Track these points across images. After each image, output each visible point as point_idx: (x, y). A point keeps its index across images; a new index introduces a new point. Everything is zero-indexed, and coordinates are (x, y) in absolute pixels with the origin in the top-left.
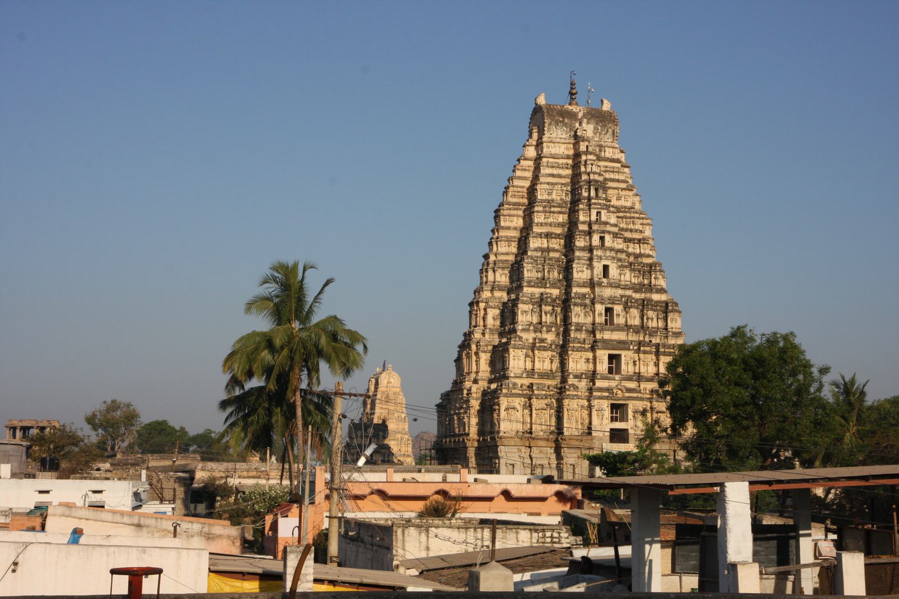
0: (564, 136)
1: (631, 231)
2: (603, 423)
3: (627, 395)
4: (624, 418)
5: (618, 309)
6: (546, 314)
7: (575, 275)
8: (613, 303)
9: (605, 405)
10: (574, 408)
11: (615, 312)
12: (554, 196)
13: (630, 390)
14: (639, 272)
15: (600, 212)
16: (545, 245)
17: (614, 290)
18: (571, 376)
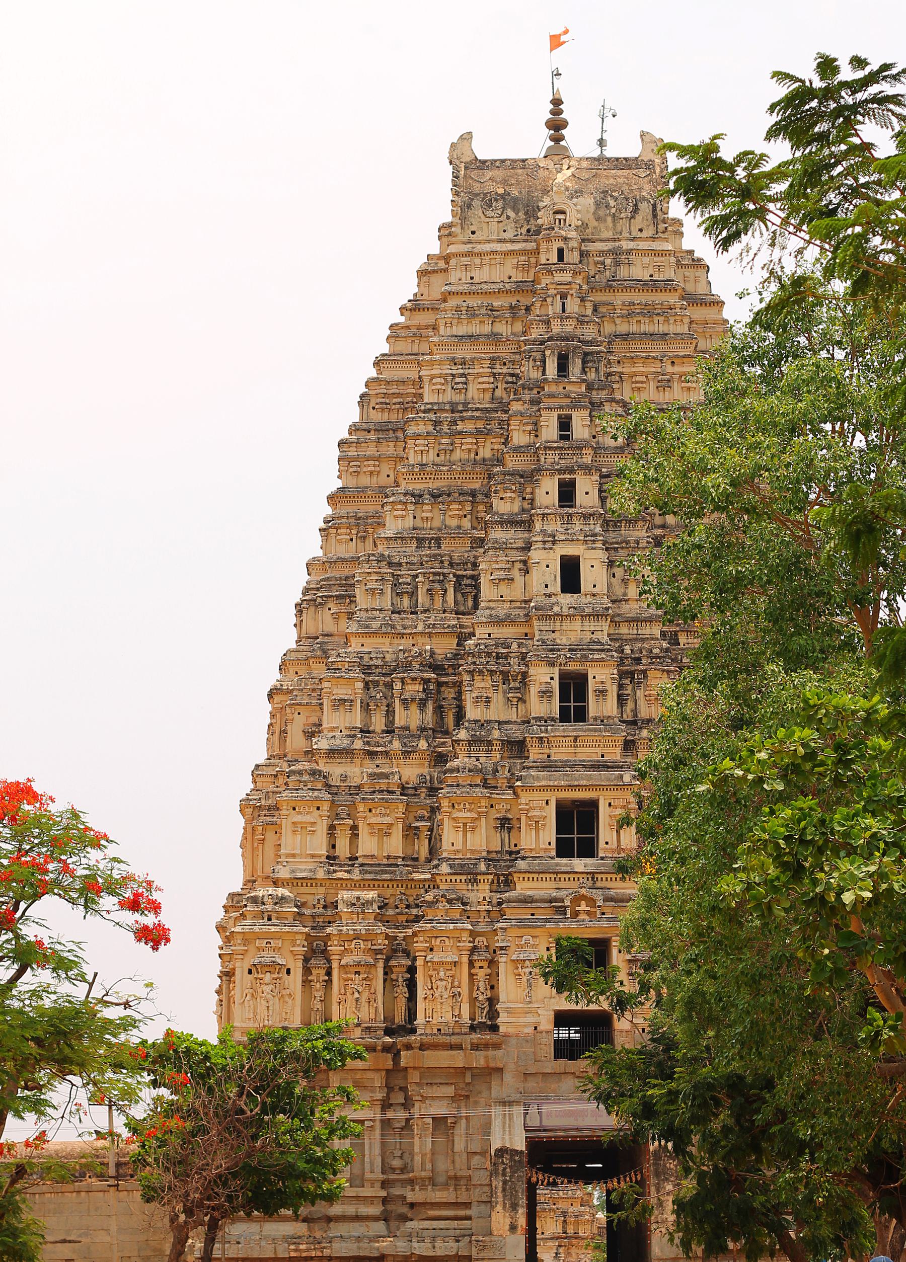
0: (509, 235)
5: (601, 676)
6: (405, 703)
7: (487, 592)
10: (442, 951)
15: (570, 417)
16: (437, 523)
18: (445, 868)
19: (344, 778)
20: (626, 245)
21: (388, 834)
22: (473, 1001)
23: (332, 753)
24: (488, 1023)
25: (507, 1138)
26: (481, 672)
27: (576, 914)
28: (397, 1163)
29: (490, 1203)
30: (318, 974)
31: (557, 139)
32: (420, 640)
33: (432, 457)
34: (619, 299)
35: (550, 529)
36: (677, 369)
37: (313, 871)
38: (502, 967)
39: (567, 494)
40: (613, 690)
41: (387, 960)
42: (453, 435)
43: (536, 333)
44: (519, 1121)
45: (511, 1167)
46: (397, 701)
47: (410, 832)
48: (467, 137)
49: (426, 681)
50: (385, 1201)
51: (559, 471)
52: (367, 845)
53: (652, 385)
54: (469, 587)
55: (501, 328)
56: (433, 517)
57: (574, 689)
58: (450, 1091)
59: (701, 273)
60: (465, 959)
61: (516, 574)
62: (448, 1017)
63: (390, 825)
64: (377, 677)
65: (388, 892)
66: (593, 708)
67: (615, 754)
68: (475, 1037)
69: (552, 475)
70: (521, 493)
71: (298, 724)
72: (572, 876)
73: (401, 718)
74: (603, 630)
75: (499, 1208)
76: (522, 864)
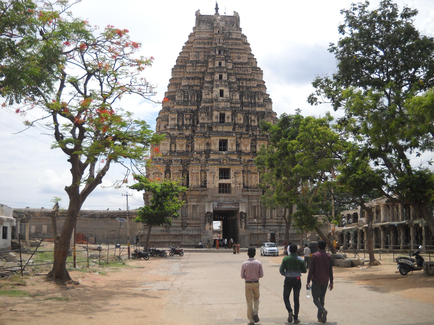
0: (208, 28)
1: (245, 74)
2: (214, 181)
3: (230, 163)
5: (228, 114)
6: (186, 119)
7: (204, 96)
8: (225, 110)
9: (216, 170)
10: (194, 170)
11: (226, 116)
12: (200, 58)
13: (233, 160)
14: (248, 96)
15: (221, 62)
16: (193, 84)
17: (226, 104)
18: (195, 153)
19: (173, 134)
20: (231, 31)
21: (183, 146)
22: (201, 181)
23: (171, 129)
24: (204, 185)
26: (203, 113)
27: (223, 163)
28: (184, 215)
29: (205, 224)
30: (168, 175)
31: (217, 11)
32: (189, 107)
33: (192, 71)
34: (230, 41)
35: (218, 84)
36: (242, 55)
37: (167, 153)
38: (207, 174)
39: (221, 77)
40: (231, 117)
41: (182, 173)
43: (214, 46)
44: (212, 206)
47: (187, 146)
48: (199, 11)
49: (191, 115)
50: (182, 223)
51: (219, 73)
52: (178, 148)
53: (237, 58)
54: (200, 96)
55: (206, 46)
56: (191, 82)
57: (222, 116)
58: (196, 200)
59: (245, 38)
60: (200, 172)
61: (210, 93)
62: (196, 184)
63: (183, 144)
64: (180, 114)
65: (182, 158)
66: (226, 121)
67: (231, 130)
68: (202, 189)
70: (211, 77)
71: (163, 124)
74: (229, 105)
75: (207, 224)
76: (212, 152)
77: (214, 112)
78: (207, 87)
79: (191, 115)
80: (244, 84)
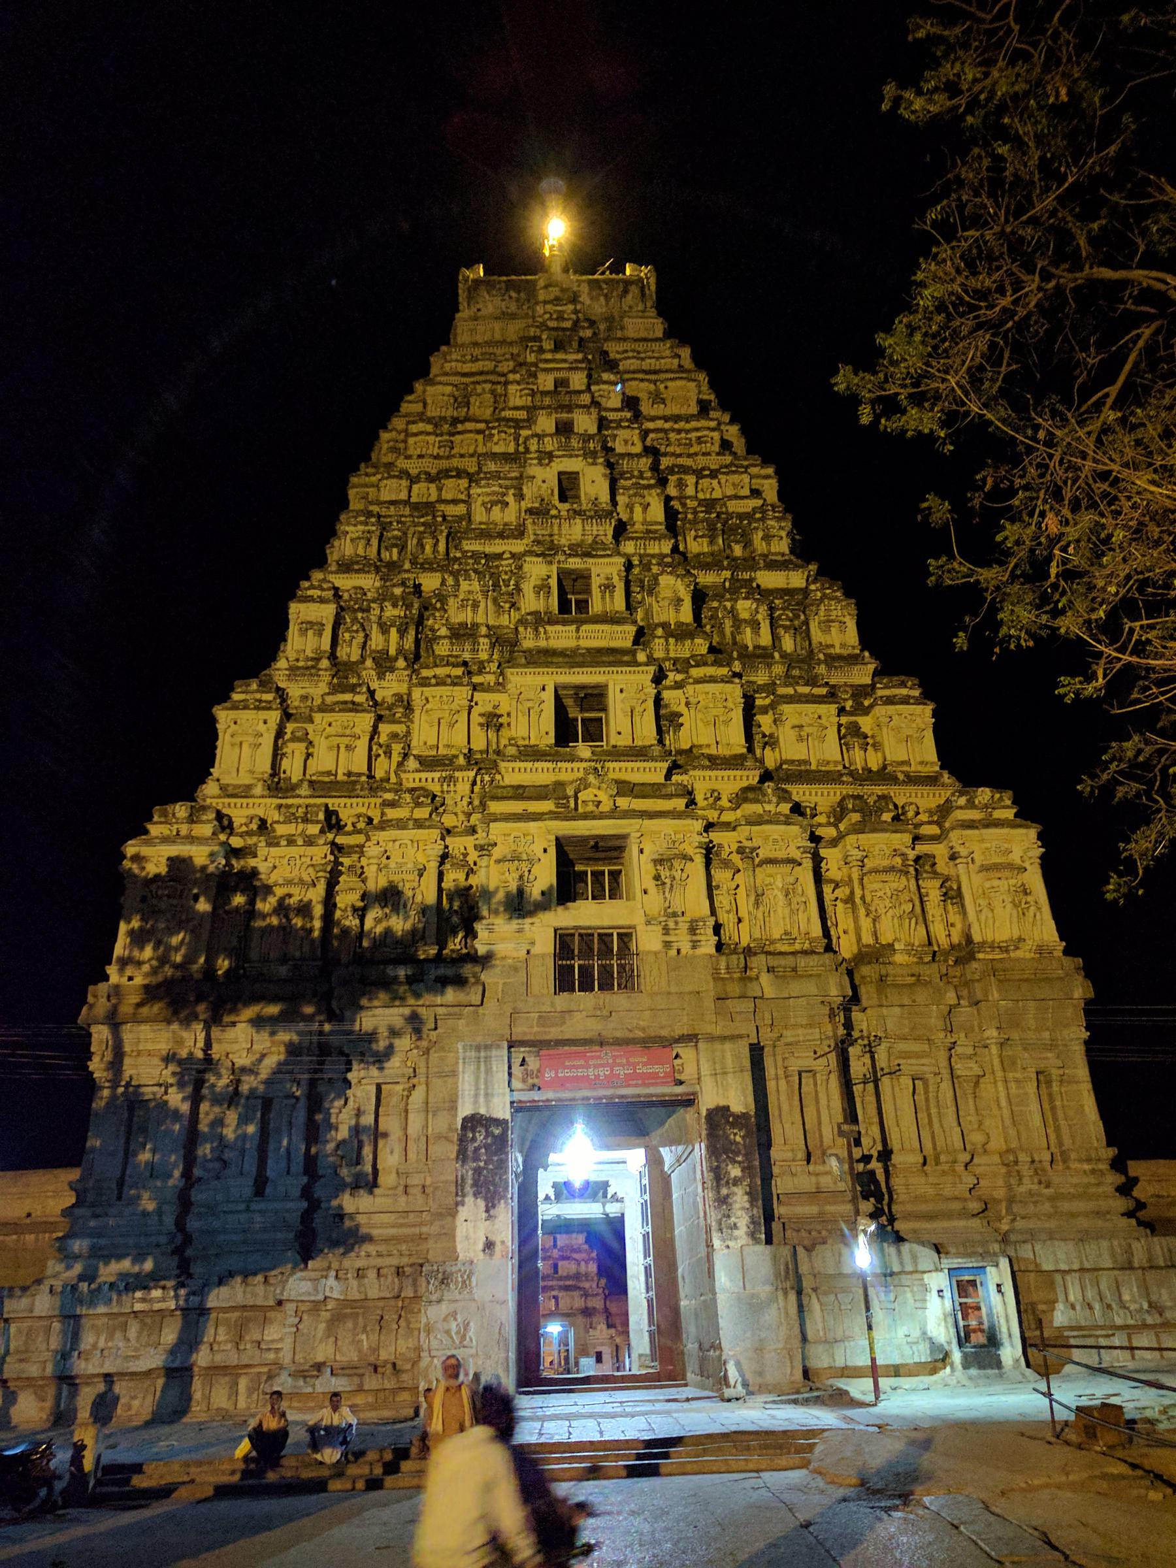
0: (513, 307)
3: (623, 803)
4: (611, 887)
5: (605, 570)
6: (384, 629)
7: (479, 515)
8: (588, 555)
11: (595, 582)
18: (412, 764)
19: (304, 698)
25: (482, 1099)
35: (549, 448)
42: (453, 434)
45: (487, 1146)
46: (375, 626)
52: (323, 761)
61: (510, 499)
69: (550, 414)
72: (575, 765)
73: (377, 641)
75: (463, 1213)
77: (526, 567)
78: (497, 476)
79: (409, 607)
80: (690, 491)
